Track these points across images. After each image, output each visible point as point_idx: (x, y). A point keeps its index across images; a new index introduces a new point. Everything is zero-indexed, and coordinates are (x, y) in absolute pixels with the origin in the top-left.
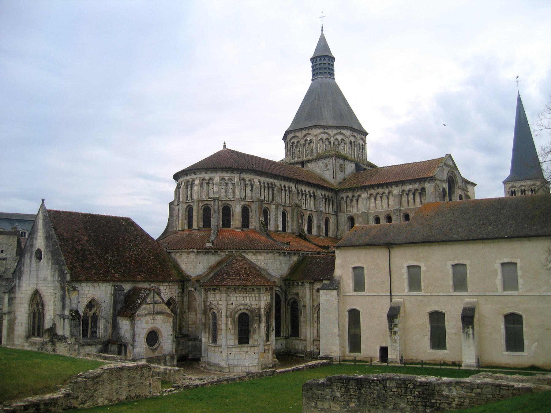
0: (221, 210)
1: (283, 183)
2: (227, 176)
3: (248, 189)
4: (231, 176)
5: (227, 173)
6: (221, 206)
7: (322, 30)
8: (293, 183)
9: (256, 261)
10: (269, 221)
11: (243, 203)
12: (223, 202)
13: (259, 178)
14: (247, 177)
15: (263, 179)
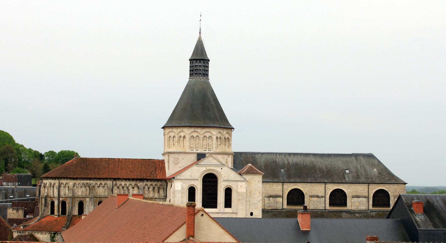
0: (50, 204)
1: (99, 182)
2: (53, 182)
3: (67, 189)
4: (55, 182)
5: (53, 180)
6: (50, 201)
7: (200, 33)
8: (111, 180)
9: (42, 238)
10: (85, 208)
11: (61, 199)
12: (50, 198)
13: (75, 181)
14: (64, 181)
15: (78, 182)
